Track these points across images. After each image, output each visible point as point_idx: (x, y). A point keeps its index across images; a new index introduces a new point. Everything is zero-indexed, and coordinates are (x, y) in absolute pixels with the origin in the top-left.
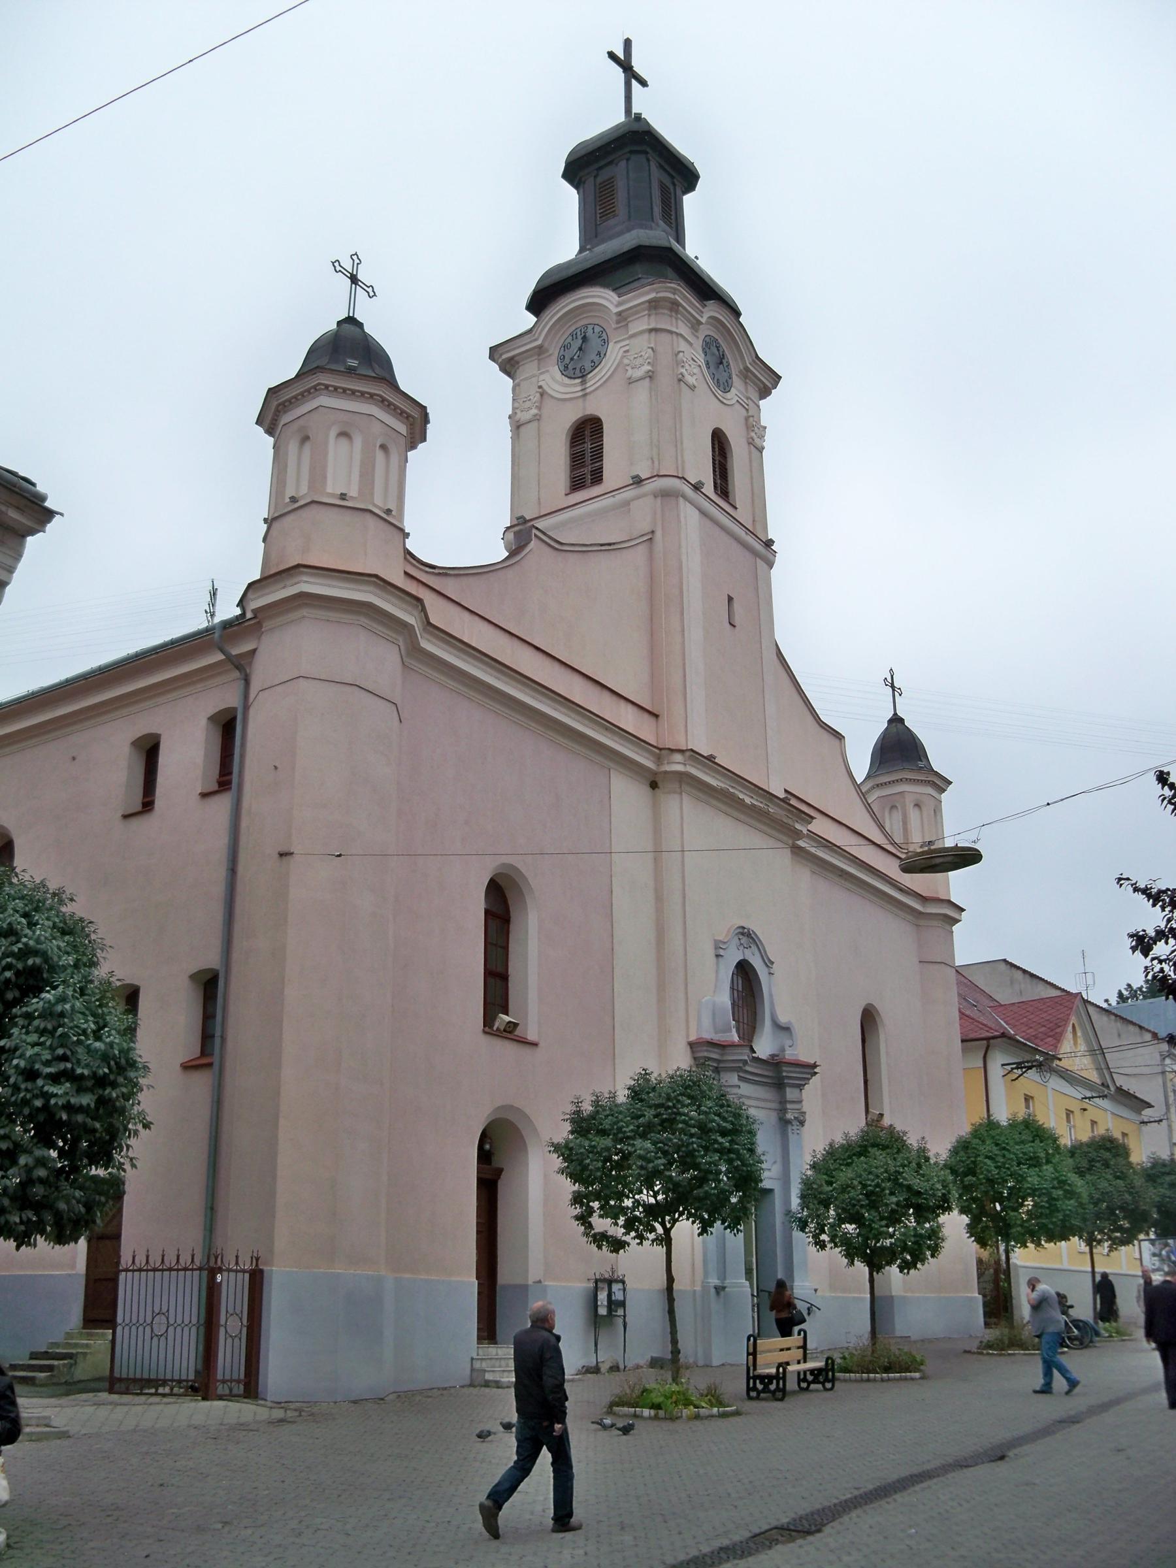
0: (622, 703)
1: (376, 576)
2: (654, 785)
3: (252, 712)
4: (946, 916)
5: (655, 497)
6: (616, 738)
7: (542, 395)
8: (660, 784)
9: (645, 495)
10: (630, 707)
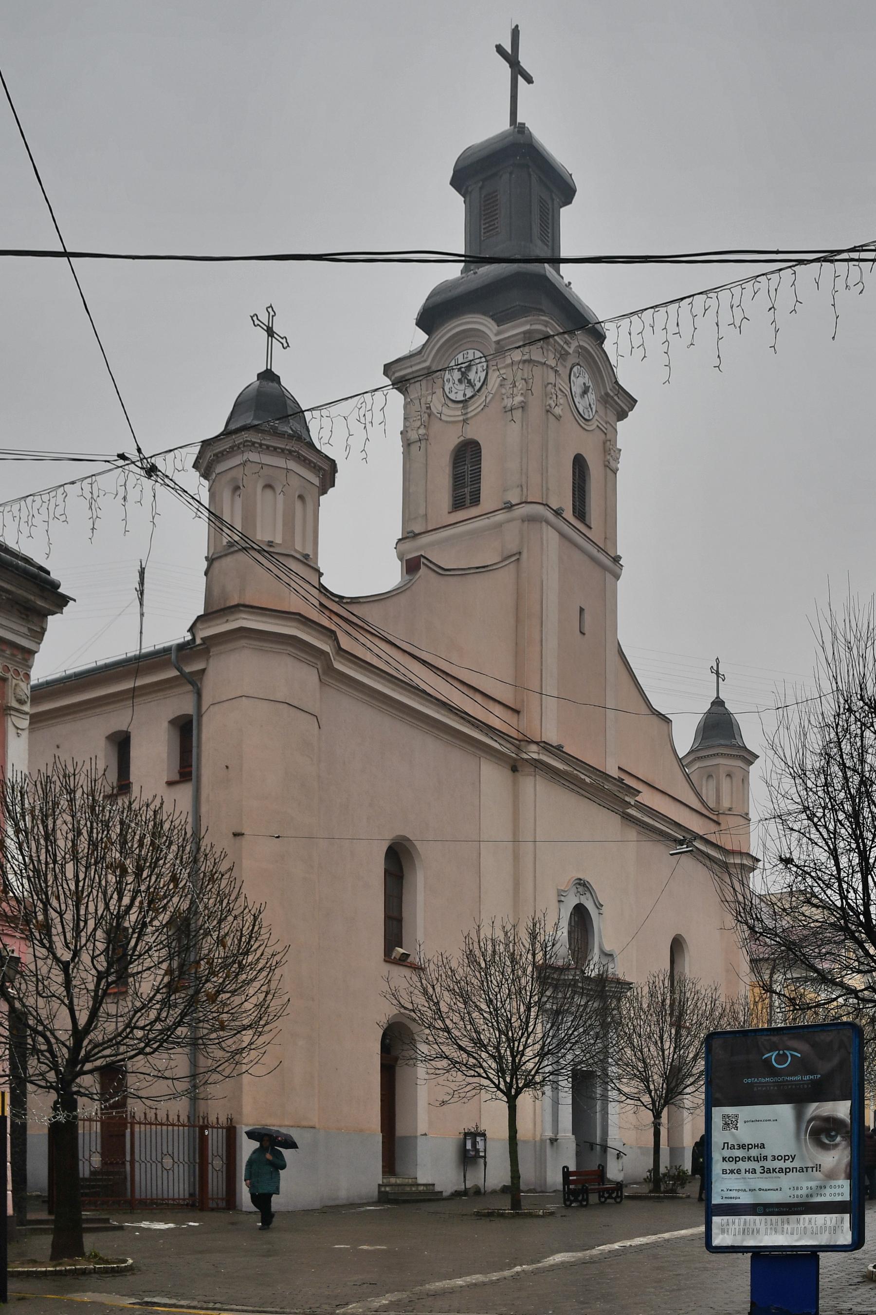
1: (299, 614)
3: (205, 719)
5: (523, 521)
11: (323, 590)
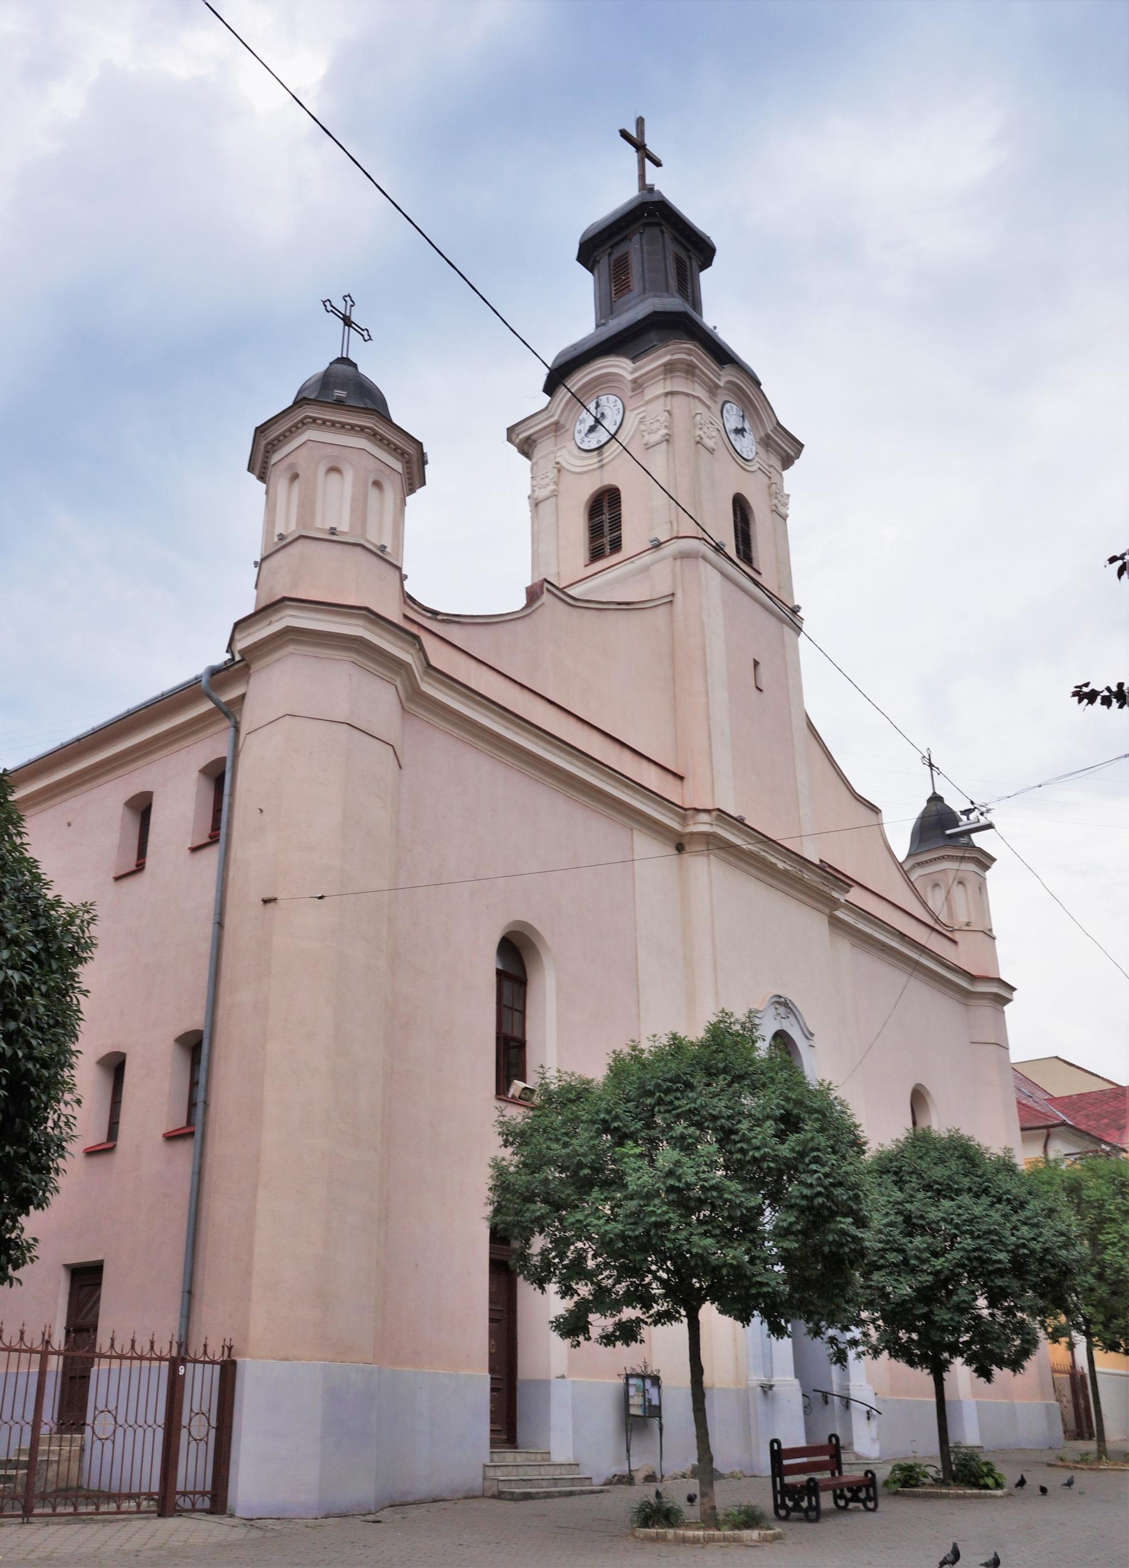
0: (645, 763)
2: (680, 848)
4: (997, 995)
5: (675, 559)
6: (637, 797)
7: (559, 471)
8: (687, 848)
9: (662, 560)
10: (653, 768)
11: (409, 599)
